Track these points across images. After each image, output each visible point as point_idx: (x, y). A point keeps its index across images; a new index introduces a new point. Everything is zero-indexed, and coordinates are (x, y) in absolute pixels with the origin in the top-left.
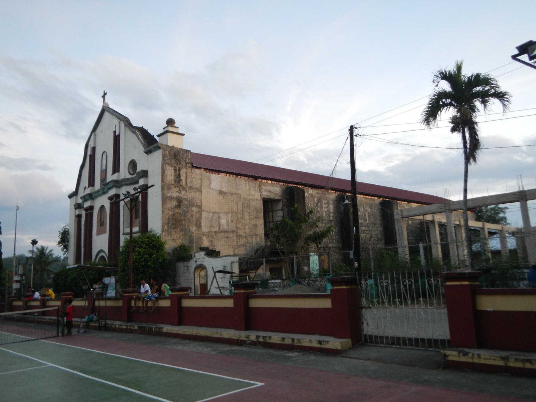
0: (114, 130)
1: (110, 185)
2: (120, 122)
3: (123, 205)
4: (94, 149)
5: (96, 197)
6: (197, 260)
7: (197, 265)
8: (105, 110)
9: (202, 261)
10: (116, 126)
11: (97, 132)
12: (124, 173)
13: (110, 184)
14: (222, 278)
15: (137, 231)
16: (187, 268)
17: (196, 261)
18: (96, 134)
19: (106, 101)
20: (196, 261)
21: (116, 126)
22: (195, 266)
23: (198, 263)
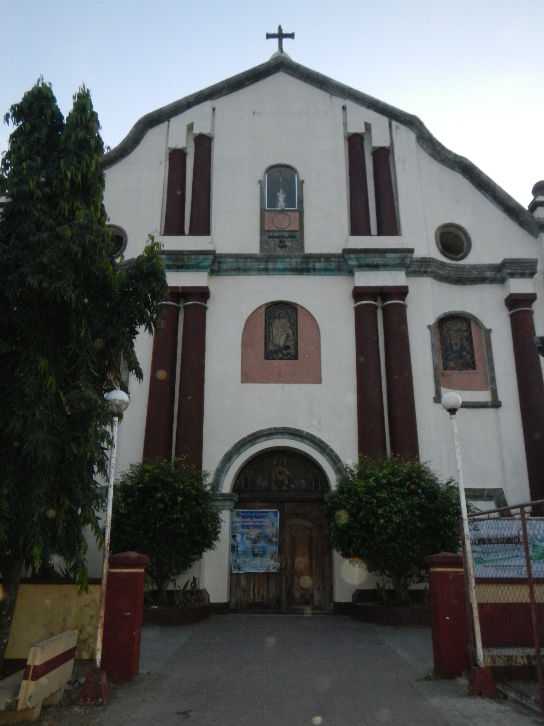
0: (361, 130)
1: (384, 257)
2: (390, 125)
11: (221, 103)
13: (388, 255)
15: (486, 402)
18: (214, 109)
19: (285, 49)
21: (368, 126)
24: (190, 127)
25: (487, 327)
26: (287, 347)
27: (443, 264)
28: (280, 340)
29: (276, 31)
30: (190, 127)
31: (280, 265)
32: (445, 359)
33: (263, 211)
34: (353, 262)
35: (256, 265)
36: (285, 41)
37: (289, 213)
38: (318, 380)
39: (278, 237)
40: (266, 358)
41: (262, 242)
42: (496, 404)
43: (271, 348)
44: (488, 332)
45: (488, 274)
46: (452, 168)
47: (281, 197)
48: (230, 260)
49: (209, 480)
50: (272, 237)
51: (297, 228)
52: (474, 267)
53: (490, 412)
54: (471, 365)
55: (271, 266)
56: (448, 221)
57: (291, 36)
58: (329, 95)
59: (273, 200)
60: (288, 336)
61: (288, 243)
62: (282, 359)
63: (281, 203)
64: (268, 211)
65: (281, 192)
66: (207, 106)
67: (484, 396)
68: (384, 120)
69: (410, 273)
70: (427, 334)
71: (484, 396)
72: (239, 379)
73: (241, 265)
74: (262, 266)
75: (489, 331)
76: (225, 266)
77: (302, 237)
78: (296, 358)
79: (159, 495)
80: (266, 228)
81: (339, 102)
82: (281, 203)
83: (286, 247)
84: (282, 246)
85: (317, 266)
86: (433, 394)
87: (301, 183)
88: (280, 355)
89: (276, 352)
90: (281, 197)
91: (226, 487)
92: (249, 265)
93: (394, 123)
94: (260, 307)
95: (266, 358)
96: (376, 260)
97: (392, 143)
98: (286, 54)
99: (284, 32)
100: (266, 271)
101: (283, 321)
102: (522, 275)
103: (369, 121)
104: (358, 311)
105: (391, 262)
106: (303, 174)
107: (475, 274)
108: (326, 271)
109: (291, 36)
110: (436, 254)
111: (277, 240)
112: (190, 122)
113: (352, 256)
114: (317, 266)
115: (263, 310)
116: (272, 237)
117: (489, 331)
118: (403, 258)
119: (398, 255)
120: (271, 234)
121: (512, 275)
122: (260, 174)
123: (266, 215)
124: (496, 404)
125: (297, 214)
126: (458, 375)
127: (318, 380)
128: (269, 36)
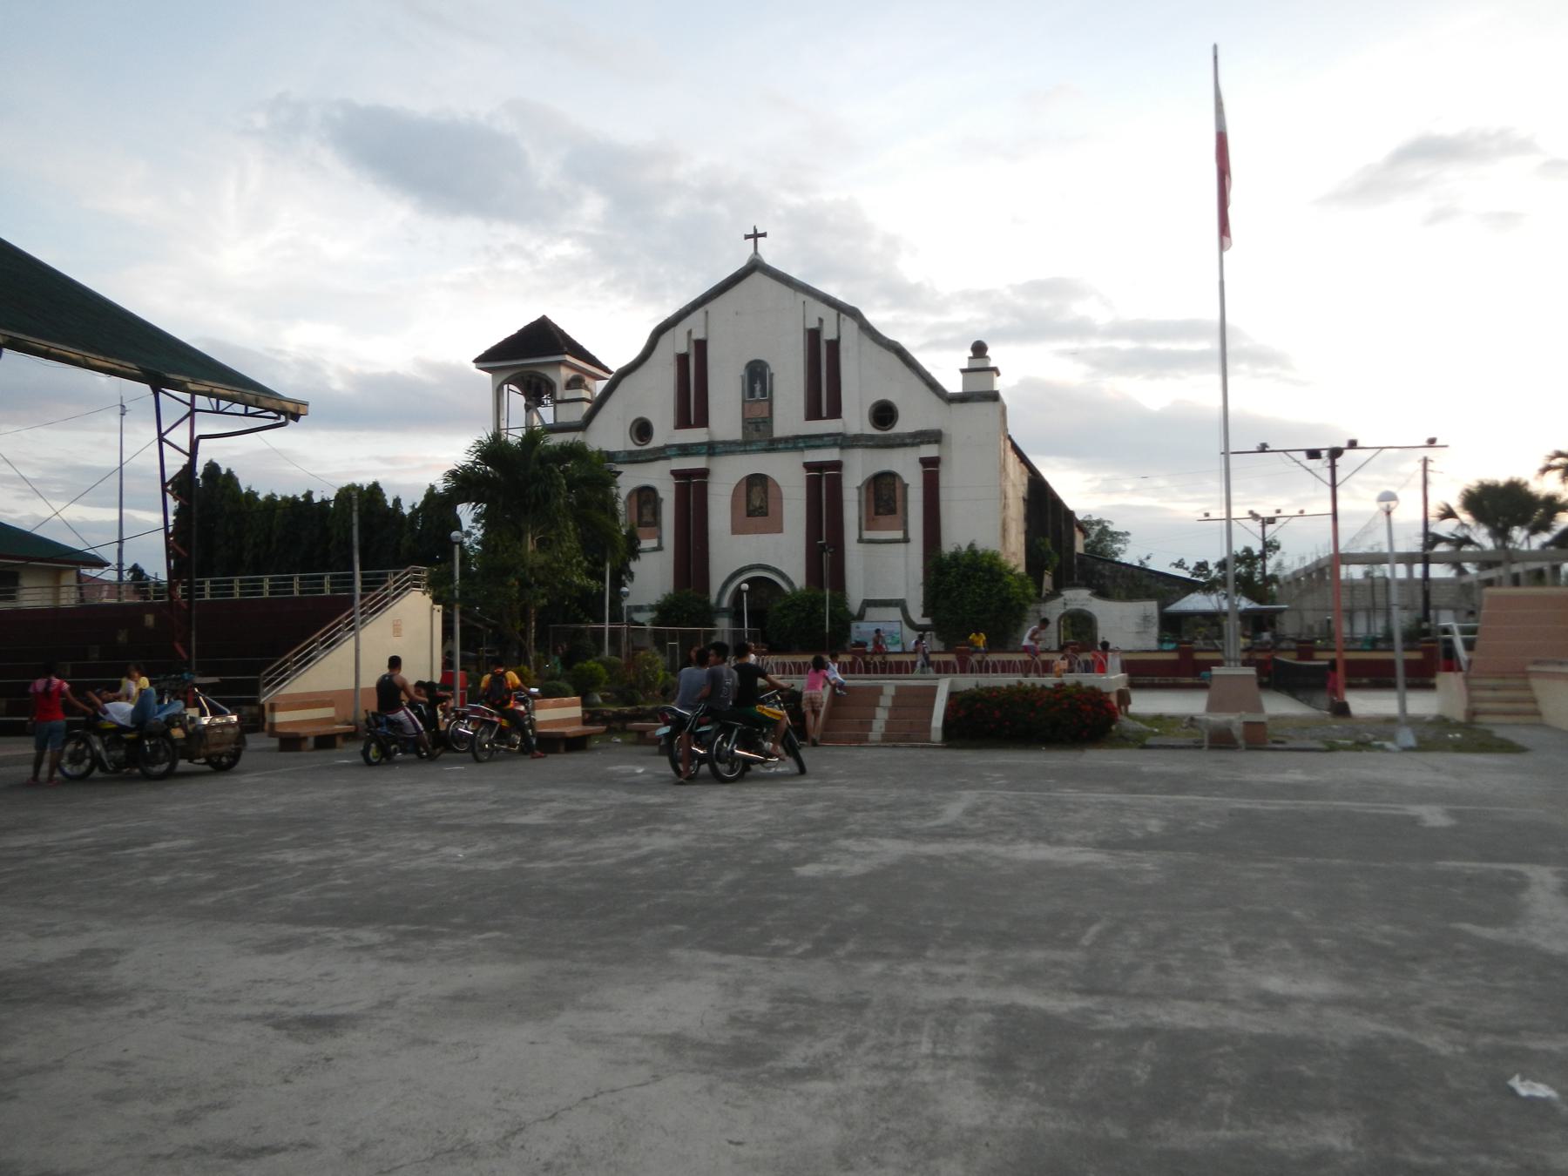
0: (814, 324)
2: (839, 315)
3: (859, 483)
4: (701, 346)
5: (727, 453)
6: (1069, 603)
7: (1069, 611)
8: (756, 266)
9: (1083, 605)
10: (821, 320)
11: (710, 306)
12: (855, 419)
13: (826, 439)
14: (1138, 633)
16: (1036, 614)
17: (1065, 604)
18: (707, 313)
19: (759, 251)
20: (1065, 604)
21: (821, 320)
22: (1062, 611)
23: (1068, 608)
24: (690, 333)
25: (906, 481)
26: (761, 507)
27: (872, 437)
28: (757, 503)
29: (752, 233)
30: (690, 333)
31: (754, 448)
32: (877, 506)
33: (744, 401)
34: (801, 445)
35: (738, 448)
36: (759, 239)
37: (762, 403)
38: (781, 531)
39: (754, 423)
40: (748, 516)
41: (744, 428)
42: (906, 540)
43: (751, 508)
44: (905, 486)
45: (908, 441)
46: (889, 350)
47: (758, 387)
48: (721, 446)
49: (713, 598)
50: (749, 423)
51: (767, 415)
52: (897, 436)
53: (903, 545)
54: (892, 511)
55: (748, 448)
56: (881, 398)
57: (764, 235)
58: (793, 291)
59: (752, 392)
60: (762, 499)
61: (761, 427)
62: (757, 516)
63: (758, 393)
64: (749, 401)
65: (758, 382)
66: (699, 314)
67: (899, 535)
68: (833, 312)
69: (842, 447)
70: (856, 492)
71: (899, 535)
72: (730, 532)
73: (728, 449)
74: (742, 449)
75: (907, 485)
76: (717, 450)
77: (771, 422)
78: (766, 514)
79: (674, 614)
80: (747, 416)
81: (802, 297)
82: (758, 393)
83: (759, 430)
84: (758, 430)
85: (780, 446)
86: (857, 537)
87: (772, 375)
88: (757, 513)
89: (754, 511)
90: (758, 387)
91: (725, 603)
92: (733, 448)
93: (842, 316)
94: (742, 479)
95: (748, 516)
96: (818, 442)
97: (839, 337)
98: (760, 257)
99: (759, 232)
100: (746, 452)
101: (759, 488)
102: (929, 442)
103: (822, 317)
104: (809, 479)
105: (828, 443)
106: (774, 367)
107: (898, 441)
108: (786, 449)
109: (764, 235)
110: (869, 430)
111: (754, 426)
112: (688, 329)
113: (800, 440)
114: (780, 446)
115: (745, 481)
116: (749, 423)
117: (907, 485)
118: (836, 440)
119: (832, 438)
120: (750, 421)
121: (922, 443)
122: (740, 370)
123: (746, 404)
124: (906, 540)
125: (767, 403)
126: (883, 519)
127: (781, 531)
128: (747, 237)
